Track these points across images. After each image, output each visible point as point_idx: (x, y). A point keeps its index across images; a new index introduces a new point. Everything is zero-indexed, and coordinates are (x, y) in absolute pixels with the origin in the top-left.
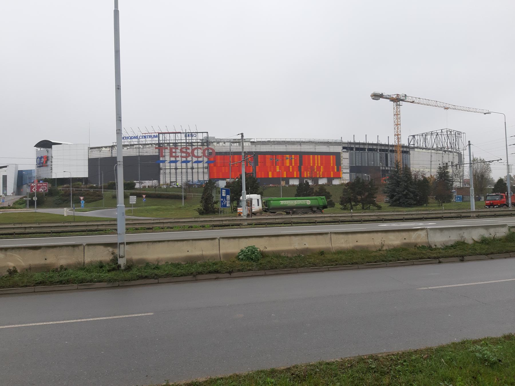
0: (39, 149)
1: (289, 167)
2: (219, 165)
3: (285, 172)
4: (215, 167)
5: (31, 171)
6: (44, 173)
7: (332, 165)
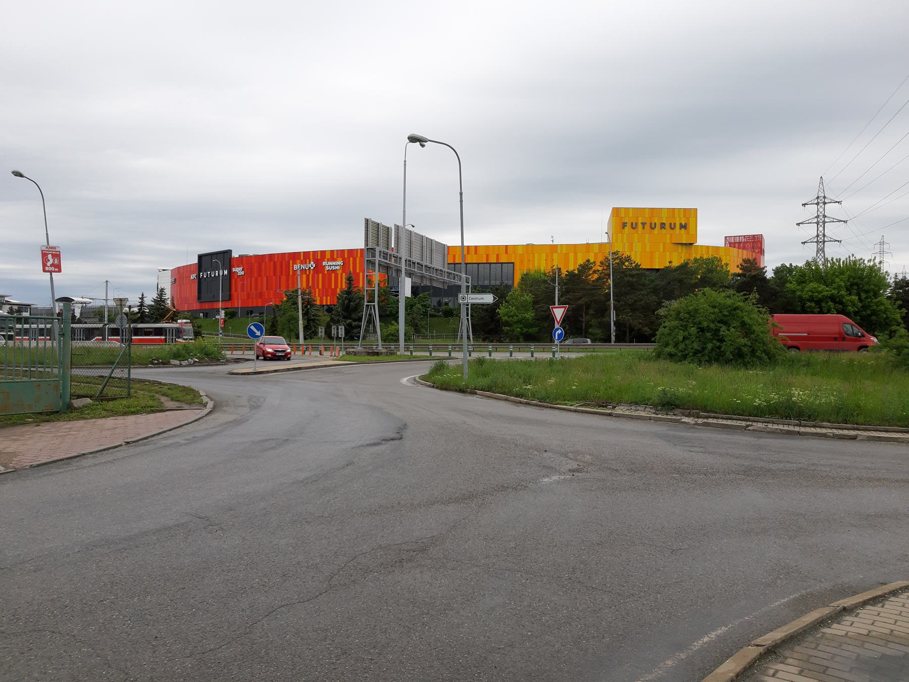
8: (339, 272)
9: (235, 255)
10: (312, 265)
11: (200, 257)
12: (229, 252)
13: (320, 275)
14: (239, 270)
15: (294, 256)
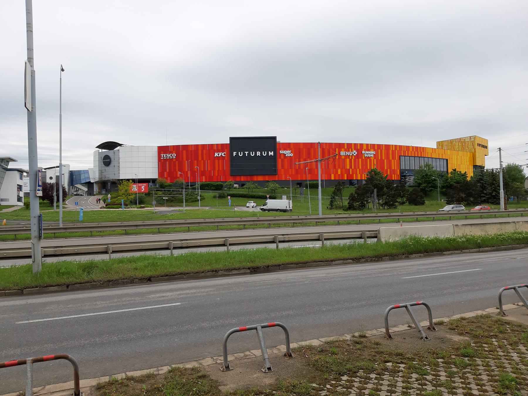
0: (100, 150)
1: (349, 170)
2: (286, 168)
3: (346, 175)
4: (283, 170)
5: (87, 172)
6: (110, 175)
7: (386, 168)
8: (372, 159)
9: (278, 140)
10: (355, 153)
11: (231, 139)
12: (275, 138)
13: (360, 160)
14: (288, 153)
15: (340, 146)
